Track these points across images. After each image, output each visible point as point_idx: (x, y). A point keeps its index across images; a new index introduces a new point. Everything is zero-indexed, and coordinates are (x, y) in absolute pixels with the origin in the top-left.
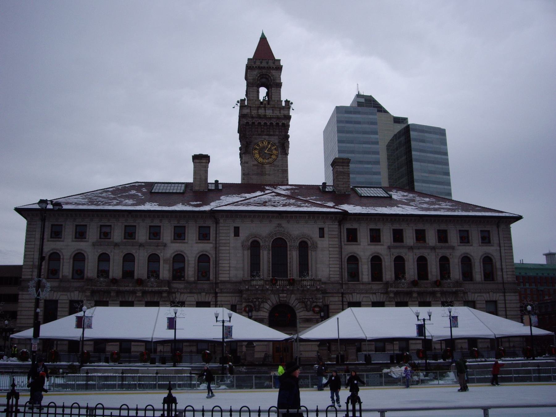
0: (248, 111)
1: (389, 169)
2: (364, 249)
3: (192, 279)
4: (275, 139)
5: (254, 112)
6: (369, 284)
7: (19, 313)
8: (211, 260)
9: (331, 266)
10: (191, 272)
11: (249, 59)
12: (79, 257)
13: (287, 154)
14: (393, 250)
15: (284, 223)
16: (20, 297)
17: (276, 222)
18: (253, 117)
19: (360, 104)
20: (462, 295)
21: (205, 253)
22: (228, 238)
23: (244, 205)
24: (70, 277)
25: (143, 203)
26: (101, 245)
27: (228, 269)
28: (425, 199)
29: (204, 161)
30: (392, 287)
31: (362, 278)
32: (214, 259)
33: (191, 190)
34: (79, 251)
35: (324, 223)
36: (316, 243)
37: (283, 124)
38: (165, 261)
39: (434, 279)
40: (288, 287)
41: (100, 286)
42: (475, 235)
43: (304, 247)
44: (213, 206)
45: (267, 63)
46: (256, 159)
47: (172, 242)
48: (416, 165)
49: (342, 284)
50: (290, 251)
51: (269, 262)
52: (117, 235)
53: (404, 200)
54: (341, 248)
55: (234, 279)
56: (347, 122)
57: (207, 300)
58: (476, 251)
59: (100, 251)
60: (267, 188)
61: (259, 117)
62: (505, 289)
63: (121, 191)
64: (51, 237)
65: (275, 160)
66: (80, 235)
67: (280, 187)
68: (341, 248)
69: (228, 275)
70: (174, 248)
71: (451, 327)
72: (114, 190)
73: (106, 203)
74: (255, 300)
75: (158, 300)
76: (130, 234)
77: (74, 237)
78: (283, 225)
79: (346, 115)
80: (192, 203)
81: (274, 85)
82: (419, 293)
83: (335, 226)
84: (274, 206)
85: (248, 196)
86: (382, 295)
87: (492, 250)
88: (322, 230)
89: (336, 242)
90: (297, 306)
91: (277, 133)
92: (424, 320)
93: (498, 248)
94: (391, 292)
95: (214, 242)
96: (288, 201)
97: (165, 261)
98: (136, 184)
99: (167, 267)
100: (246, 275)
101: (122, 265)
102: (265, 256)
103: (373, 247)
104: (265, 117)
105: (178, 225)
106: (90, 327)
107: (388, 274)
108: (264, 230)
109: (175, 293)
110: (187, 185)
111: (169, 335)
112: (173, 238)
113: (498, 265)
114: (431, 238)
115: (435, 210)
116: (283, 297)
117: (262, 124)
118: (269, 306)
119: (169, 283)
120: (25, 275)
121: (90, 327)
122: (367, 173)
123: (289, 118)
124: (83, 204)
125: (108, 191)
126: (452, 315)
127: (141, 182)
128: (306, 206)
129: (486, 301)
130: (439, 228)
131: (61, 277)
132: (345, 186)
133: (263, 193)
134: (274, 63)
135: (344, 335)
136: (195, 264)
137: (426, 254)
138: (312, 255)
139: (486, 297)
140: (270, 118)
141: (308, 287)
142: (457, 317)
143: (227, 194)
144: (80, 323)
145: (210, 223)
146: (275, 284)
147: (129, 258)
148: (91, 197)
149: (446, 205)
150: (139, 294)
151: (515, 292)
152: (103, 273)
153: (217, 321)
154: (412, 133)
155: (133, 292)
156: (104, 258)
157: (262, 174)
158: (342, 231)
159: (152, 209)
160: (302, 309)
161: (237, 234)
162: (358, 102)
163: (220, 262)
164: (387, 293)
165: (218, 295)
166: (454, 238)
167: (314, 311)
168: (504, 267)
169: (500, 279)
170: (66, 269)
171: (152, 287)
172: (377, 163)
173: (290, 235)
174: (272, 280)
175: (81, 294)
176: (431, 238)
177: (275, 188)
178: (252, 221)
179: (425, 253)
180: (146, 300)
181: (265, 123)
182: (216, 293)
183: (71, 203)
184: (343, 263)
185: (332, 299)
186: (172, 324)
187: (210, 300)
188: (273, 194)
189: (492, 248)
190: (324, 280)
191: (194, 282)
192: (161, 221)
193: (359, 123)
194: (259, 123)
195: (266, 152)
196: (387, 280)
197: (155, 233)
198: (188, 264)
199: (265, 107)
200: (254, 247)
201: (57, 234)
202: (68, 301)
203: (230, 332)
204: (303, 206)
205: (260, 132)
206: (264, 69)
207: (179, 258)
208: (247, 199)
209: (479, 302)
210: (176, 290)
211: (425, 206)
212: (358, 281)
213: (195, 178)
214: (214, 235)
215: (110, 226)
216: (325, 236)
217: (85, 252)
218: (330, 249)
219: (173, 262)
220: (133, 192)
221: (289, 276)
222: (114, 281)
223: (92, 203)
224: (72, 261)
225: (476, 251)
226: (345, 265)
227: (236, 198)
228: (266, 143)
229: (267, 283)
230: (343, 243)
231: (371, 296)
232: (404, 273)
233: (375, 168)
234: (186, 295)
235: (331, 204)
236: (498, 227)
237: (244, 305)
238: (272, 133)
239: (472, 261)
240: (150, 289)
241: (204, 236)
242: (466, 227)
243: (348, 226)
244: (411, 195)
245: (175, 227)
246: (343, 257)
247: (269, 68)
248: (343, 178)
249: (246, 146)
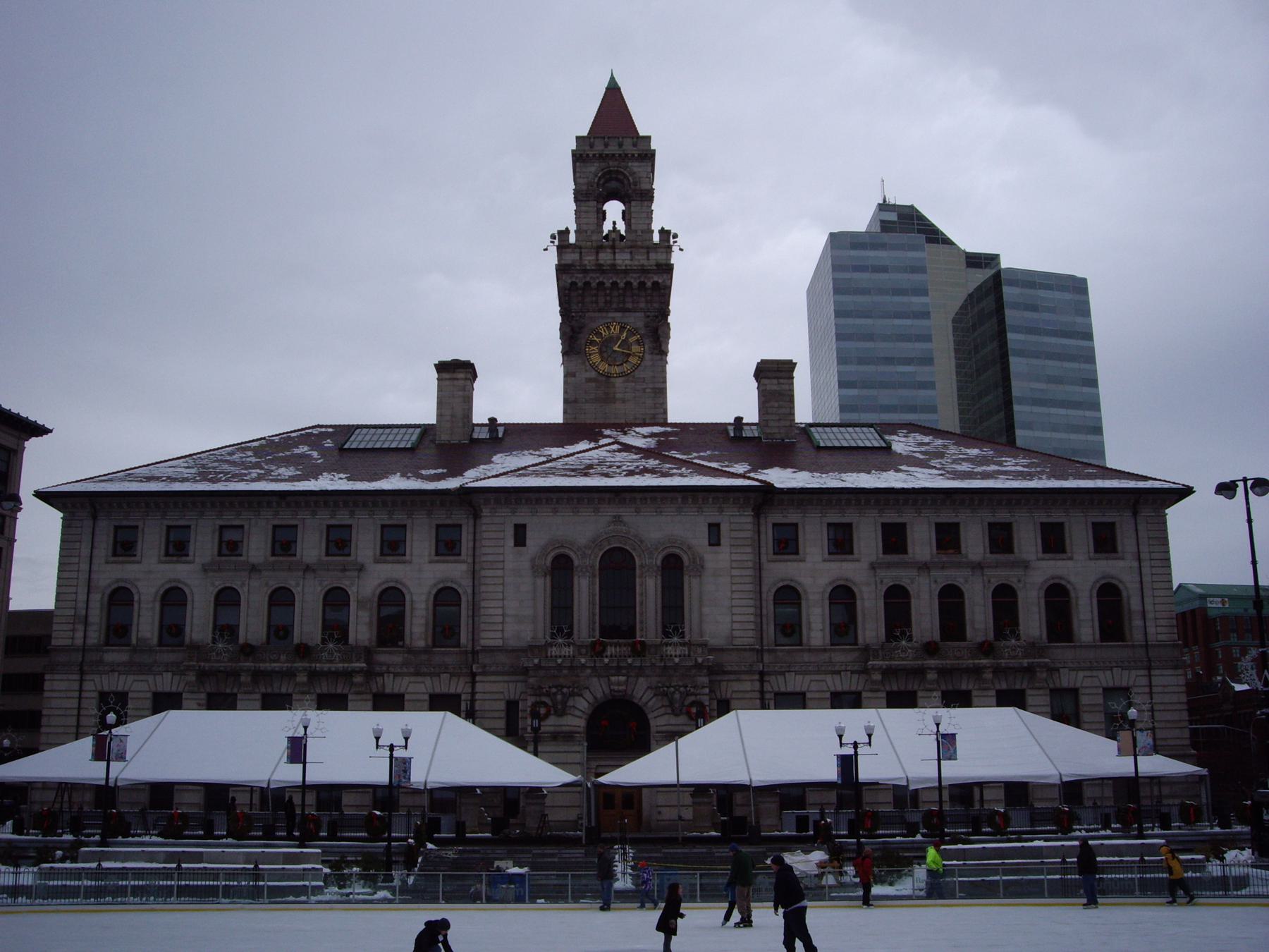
0: (576, 256)
1: (958, 373)
2: (814, 571)
3: (421, 643)
4: (636, 320)
5: (589, 259)
6: (825, 650)
7: (44, 721)
8: (464, 599)
9: (735, 610)
10: (417, 627)
11: (578, 138)
12: (173, 598)
13: (664, 353)
14: (882, 573)
15: (627, 514)
16: (47, 685)
17: (609, 511)
18: (585, 271)
19: (886, 226)
20: (1044, 675)
21: (449, 584)
22: (501, 550)
23: (537, 475)
24: (155, 641)
25: (314, 473)
26: (220, 570)
27: (499, 619)
28: (968, 451)
29: (462, 376)
30: (876, 657)
31: (809, 638)
32: (470, 598)
33: (433, 441)
34: (173, 584)
35: (721, 510)
36: (702, 559)
37: (656, 284)
38: (361, 604)
39: (980, 639)
40: (630, 661)
41: (218, 661)
42: (1079, 534)
43: (674, 568)
44: (472, 477)
45: (620, 145)
46: (594, 367)
47: (377, 562)
48: (1016, 364)
49: (760, 652)
50: (641, 576)
51: (591, 603)
52: (257, 546)
53: (917, 455)
54: (759, 568)
55: (513, 643)
56: (857, 269)
57: (452, 691)
58: (1081, 571)
59: (219, 584)
60: (607, 432)
61: (600, 269)
62: (1149, 660)
63: (273, 450)
64: (115, 554)
65: (637, 367)
66: (177, 548)
67: (638, 429)
68: (759, 568)
69: (499, 635)
70: (381, 574)
71: (939, 760)
72: (261, 445)
73: (234, 476)
74: (554, 690)
75: (345, 691)
76: (283, 544)
77: (163, 552)
78: (625, 519)
79: (854, 253)
80: (423, 472)
81: (638, 196)
82: (943, 672)
83: (746, 518)
84: (607, 475)
85: (555, 452)
86: (856, 676)
87: (1120, 569)
88: (714, 529)
89: (747, 555)
90: (650, 704)
91: (642, 305)
92: (855, 745)
93: (1136, 564)
94: (874, 668)
95: (470, 560)
96: (642, 463)
97: (361, 604)
98: (315, 431)
99: (365, 616)
100: (540, 635)
101: (266, 613)
102: (585, 590)
103: (833, 565)
104: (613, 268)
105: (390, 522)
106: (121, 757)
107: (871, 628)
108: (582, 531)
109: (382, 674)
110: (426, 430)
111: (291, 774)
112: (378, 552)
113: (1135, 604)
114: (974, 542)
115: (985, 476)
116: (619, 684)
117: (608, 284)
118: (586, 704)
119: (368, 653)
120: (61, 636)
121: (121, 757)
122: (904, 385)
123: (668, 269)
124: (184, 480)
125: (249, 449)
126: (942, 730)
127: (326, 426)
128: (681, 475)
129: (1105, 689)
130: (992, 520)
131: (134, 641)
132: (783, 423)
133: (592, 445)
134: (635, 145)
135: (688, 777)
136: (427, 609)
137: (962, 580)
138: (691, 585)
139: (1106, 678)
140: (626, 272)
141: (677, 660)
142: (954, 735)
143: (509, 450)
144: (102, 752)
145: (459, 516)
146: (601, 654)
147: (281, 599)
148: (203, 463)
149: (1016, 464)
150: (302, 678)
151: (1176, 668)
152: (226, 630)
153: (377, 746)
154: (1006, 290)
155: (290, 674)
156: (227, 599)
157: (608, 399)
158: (763, 529)
159: (330, 488)
160: (662, 711)
162: (882, 222)
163: (483, 604)
164: (865, 671)
165: (478, 678)
166: (1027, 540)
167: (688, 713)
168: (1149, 607)
169: (1138, 637)
170: (146, 624)
171: (331, 662)
172: (928, 360)
173: (642, 542)
174: (593, 645)
175: (177, 678)
176: (974, 542)
177: (625, 433)
178: (555, 511)
179: (957, 577)
180: (319, 691)
181: (615, 284)
182: (473, 675)
183: (157, 479)
184: (764, 604)
185: (736, 686)
186: (297, 750)
187: (459, 691)
188: (615, 447)
189: (1121, 563)
190: (713, 642)
191: (426, 651)
192: (352, 514)
193: (884, 269)
194: (601, 284)
195: (616, 348)
196: (868, 641)
197: (339, 542)
198: (412, 609)
199: (613, 247)
200: (560, 569)
201: (125, 547)
202: (149, 695)
203: (405, 771)
204: (672, 475)
205: (601, 305)
206: (614, 158)
207: (392, 597)
208: (555, 460)
209: (1087, 691)
210: (384, 668)
211: (965, 467)
212: (801, 644)
213: (440, 415)
214: (471, 544)
215: (242, 527)
216: (722, 541)
217: (186, 585)
218: (735, 572)
219: (379, 606)
220: (303, 449)
221: (638, 633)
222: (248, 650)
223: (203, 476)
224: (158, 606)
225: (1081, 571)
226: (769, 607)
227: (527, 459)
228: (615, 330)
229: (584, 651)
230: (764, 558)
231: (829, 678)
232: (908, 624)
233: (922, 372)
234: (407, 679)
235: (740, 468)
236: (1135, 514)
237: (531, 700)
238: (629, 306)
239: (1073, 595)
240: (326, 666)
241: (447, 546)
242: (1056, 516)
243: (776, 517)
244: (939, 442)
245: (383, 526)
246: (765, 589)
247: (625, 157)
248: (779, 407)
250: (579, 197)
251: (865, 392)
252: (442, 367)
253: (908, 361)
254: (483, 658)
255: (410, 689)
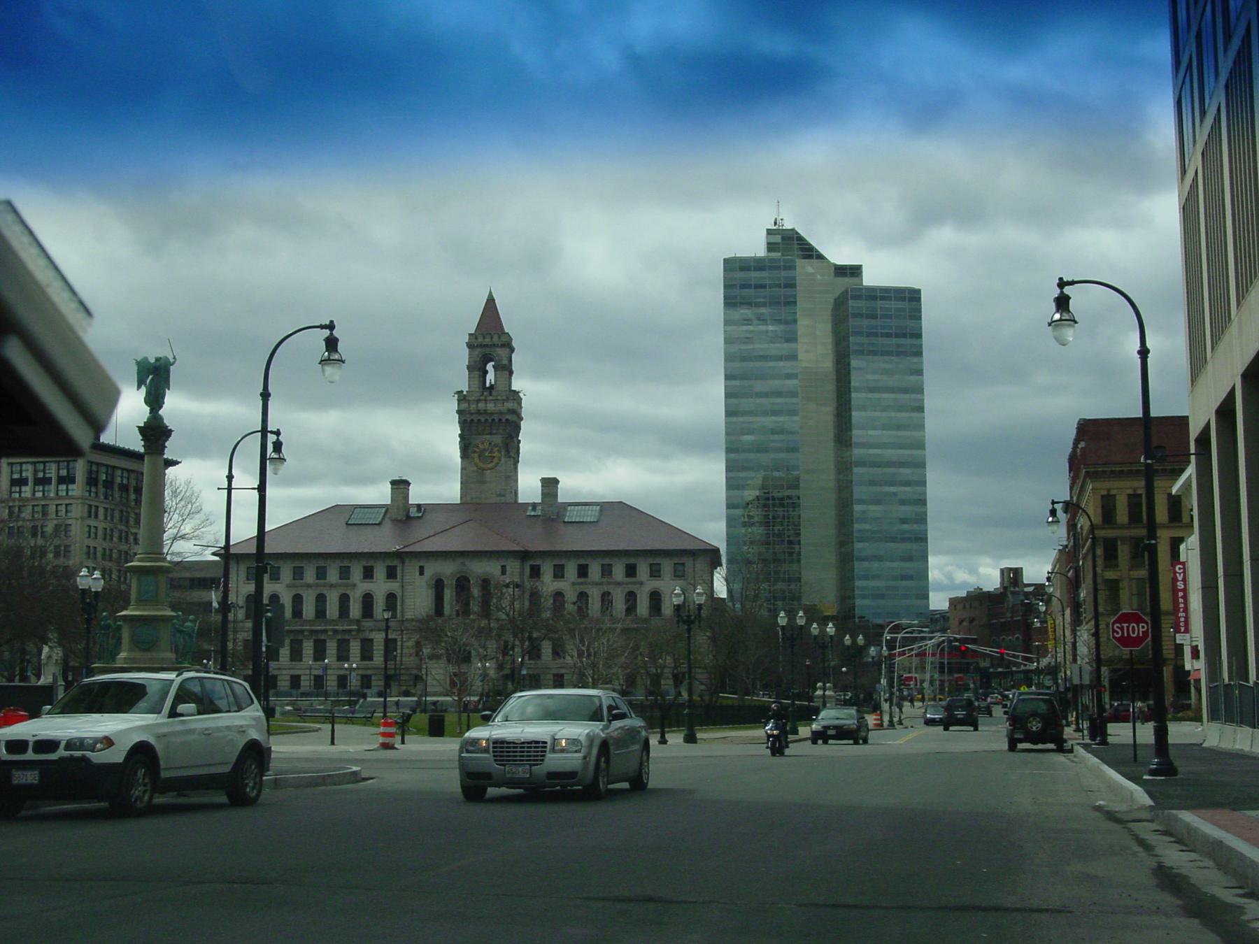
4: (497, 439)
15: (468, 562)
19: (771, 247)
59: (294, 592)
61: (479, 412)
70: (364, 587)
88: (504, 568)
108: (448, 569)
119: (358, 622)
140: (492, 414)
147: (321, 599)
161: (422, 573)
162: (768, 244)
200: (439, 585)
241: (391, 574)
247: (495, 346)
250: (470, 368)
251: (746, 383)
252: (393, 483)
253: (780, 358)
254: (406, 624)
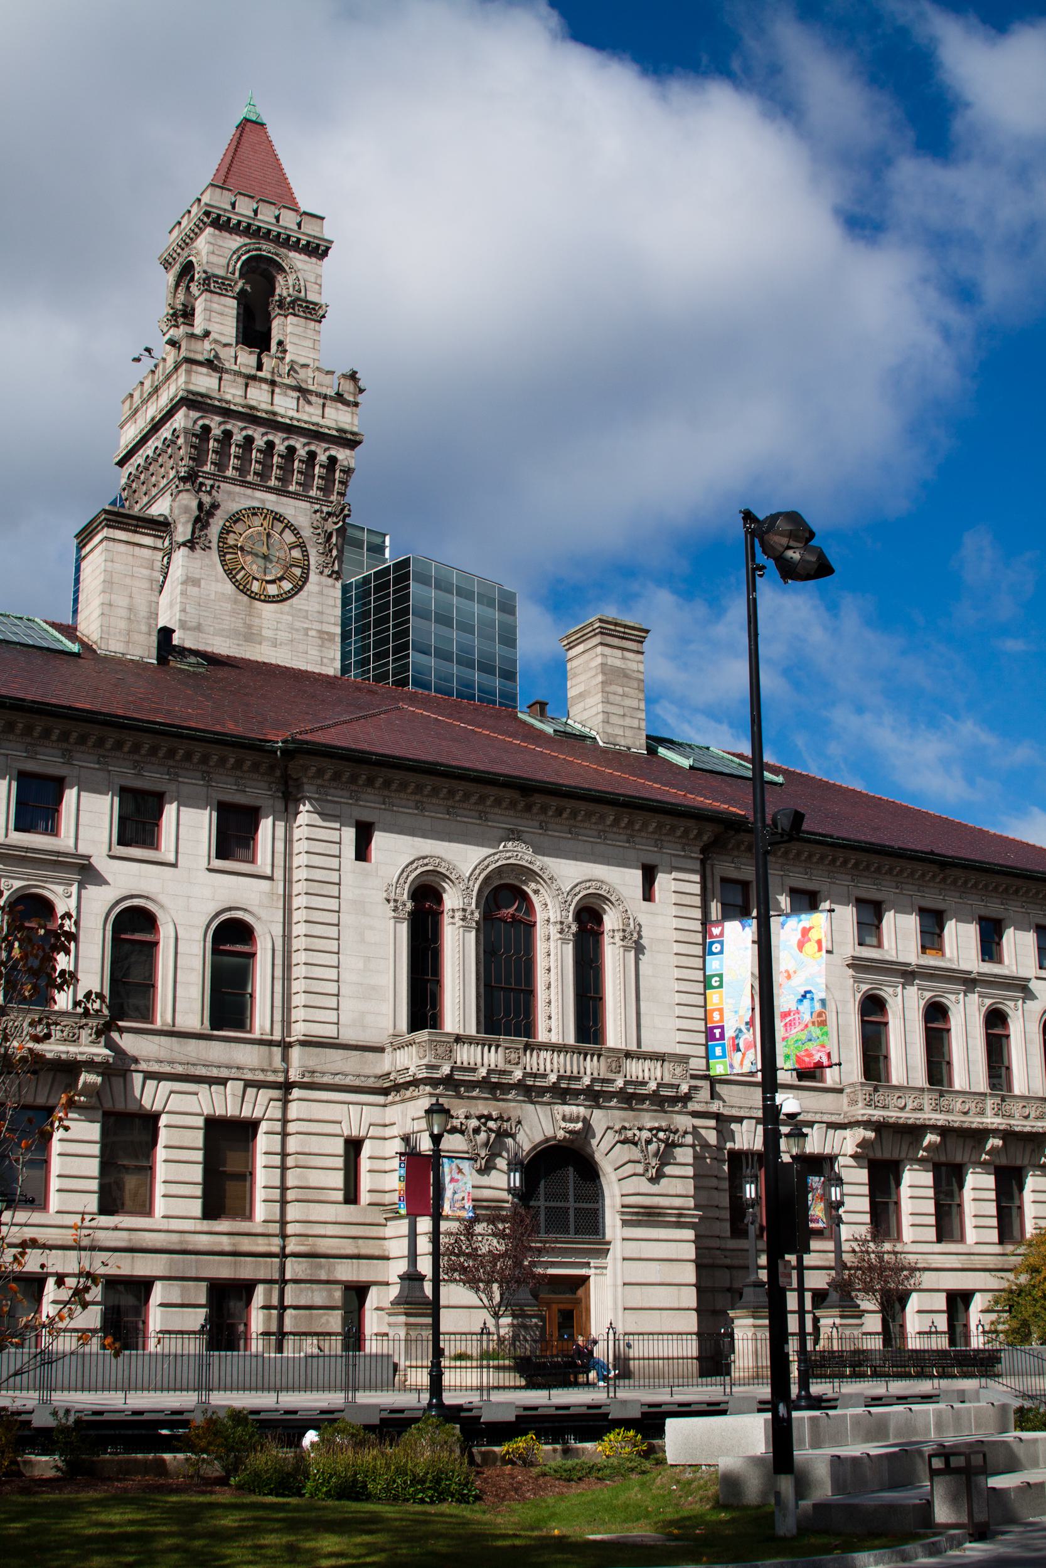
61: (251, 417)
132: (628, 722)
182: (287, 1087)
247: (286, 242)
249: (197, 520)
255: (175, 1103)
